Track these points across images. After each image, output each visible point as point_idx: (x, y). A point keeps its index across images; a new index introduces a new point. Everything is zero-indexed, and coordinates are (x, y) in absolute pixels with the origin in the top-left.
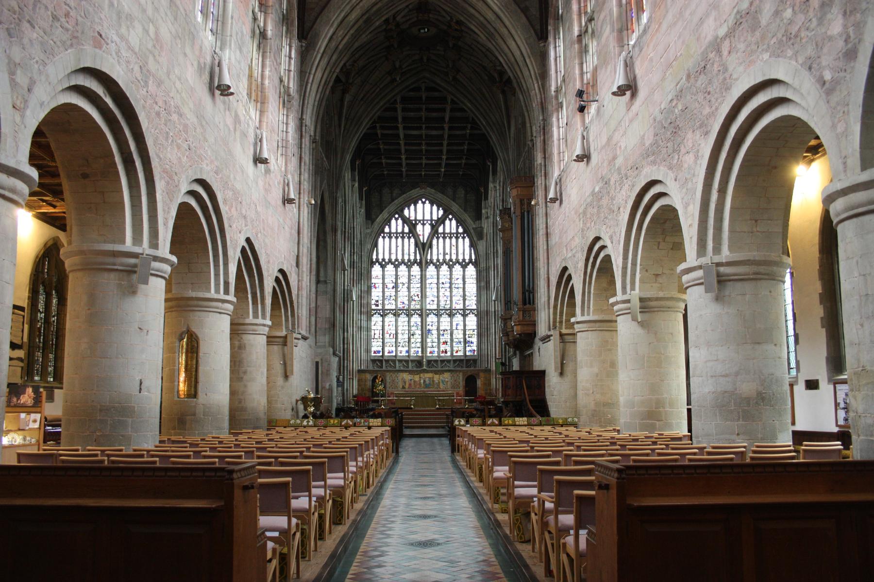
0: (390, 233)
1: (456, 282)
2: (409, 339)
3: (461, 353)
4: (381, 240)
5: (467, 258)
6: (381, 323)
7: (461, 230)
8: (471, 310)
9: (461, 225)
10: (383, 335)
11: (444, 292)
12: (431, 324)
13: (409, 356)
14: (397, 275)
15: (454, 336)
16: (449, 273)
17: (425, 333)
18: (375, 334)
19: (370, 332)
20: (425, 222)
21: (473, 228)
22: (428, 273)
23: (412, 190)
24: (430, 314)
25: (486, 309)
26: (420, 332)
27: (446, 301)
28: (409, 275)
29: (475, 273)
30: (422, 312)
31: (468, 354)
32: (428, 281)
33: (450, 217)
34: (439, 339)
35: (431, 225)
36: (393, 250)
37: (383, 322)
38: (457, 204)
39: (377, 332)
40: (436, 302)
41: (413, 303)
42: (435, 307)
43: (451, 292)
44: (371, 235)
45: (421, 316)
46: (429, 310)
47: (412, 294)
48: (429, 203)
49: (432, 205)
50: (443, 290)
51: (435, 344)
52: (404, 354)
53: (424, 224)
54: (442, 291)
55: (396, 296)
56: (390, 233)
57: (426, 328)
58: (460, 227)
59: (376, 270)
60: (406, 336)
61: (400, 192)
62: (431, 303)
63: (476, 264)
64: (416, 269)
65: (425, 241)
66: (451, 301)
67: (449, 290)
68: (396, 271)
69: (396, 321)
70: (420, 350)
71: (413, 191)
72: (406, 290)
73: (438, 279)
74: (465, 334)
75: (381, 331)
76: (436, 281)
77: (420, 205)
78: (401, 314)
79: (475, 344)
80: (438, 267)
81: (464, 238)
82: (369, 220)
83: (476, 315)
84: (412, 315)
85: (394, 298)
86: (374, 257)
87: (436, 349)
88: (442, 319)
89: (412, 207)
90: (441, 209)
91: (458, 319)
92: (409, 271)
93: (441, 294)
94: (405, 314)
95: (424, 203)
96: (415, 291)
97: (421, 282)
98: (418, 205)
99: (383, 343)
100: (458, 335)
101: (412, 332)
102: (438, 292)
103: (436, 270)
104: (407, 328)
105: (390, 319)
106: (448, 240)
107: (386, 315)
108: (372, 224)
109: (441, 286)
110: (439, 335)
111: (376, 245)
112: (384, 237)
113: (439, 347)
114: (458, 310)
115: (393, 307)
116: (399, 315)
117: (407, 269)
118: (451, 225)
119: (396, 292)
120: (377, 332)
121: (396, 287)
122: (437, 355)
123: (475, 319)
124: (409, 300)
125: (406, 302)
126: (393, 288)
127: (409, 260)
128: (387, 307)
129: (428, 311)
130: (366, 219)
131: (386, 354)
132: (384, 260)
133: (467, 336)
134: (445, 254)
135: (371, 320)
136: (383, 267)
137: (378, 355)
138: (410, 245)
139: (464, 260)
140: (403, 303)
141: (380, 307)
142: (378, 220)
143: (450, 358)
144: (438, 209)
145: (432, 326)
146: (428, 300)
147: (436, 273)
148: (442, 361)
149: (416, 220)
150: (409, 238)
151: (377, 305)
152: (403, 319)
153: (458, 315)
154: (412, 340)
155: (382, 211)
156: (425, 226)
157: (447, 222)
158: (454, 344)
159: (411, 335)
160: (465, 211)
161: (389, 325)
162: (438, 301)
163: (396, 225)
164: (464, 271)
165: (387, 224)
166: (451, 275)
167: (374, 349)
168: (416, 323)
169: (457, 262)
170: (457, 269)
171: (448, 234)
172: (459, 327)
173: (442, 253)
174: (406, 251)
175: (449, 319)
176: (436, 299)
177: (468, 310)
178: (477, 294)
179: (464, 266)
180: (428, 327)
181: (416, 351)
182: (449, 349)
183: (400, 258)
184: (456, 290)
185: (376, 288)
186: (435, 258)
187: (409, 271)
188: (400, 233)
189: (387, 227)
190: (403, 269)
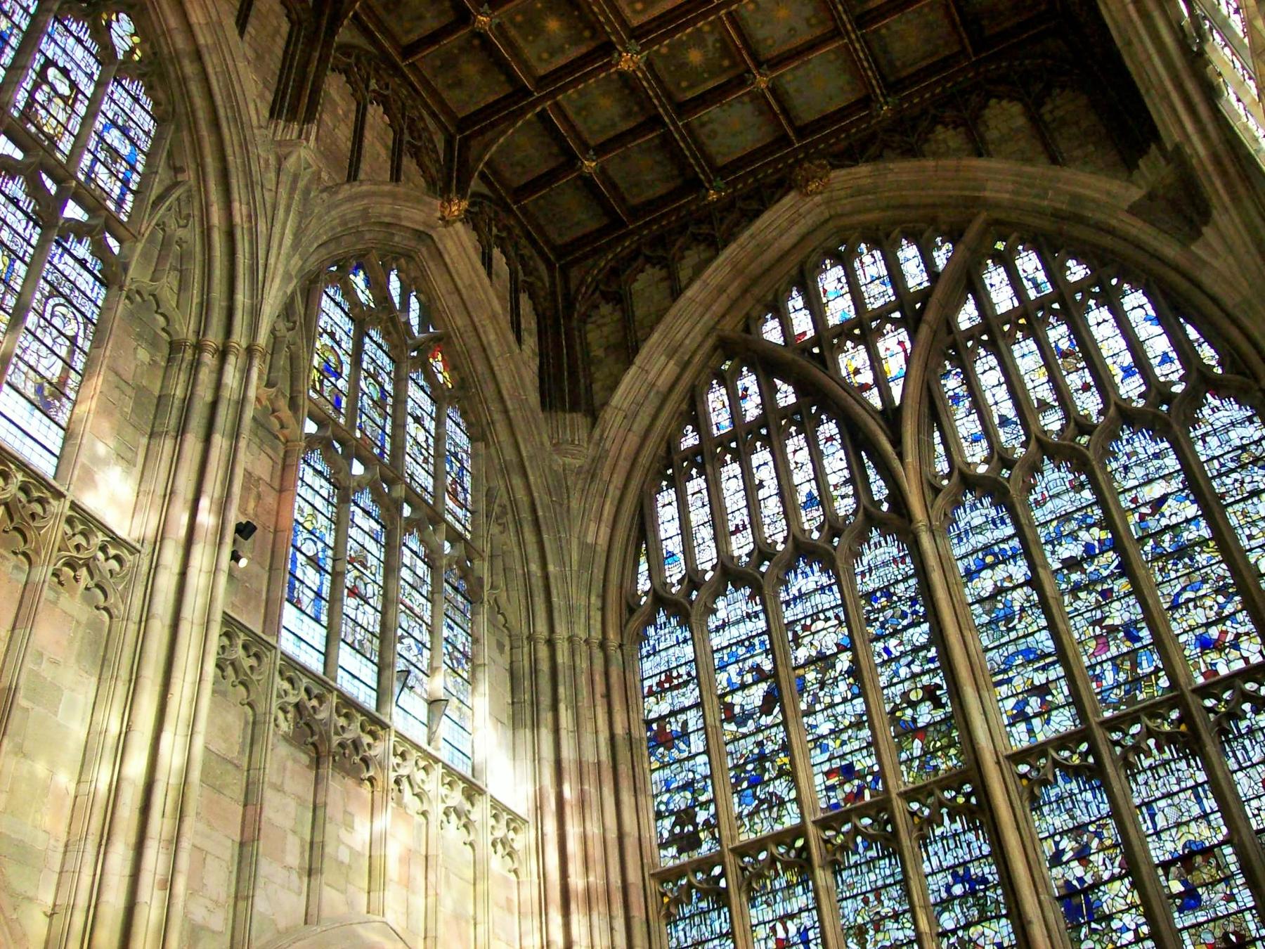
1: (1153, 524)
16: (1087, 494)
21: (1134, 210)
23: (757, 214)
27: (1132, 655)
30: (982, 790)
40: (1061, 694)
50: (1088, 599)
53: (868, 339)
62: (1034, 704)
71: (766, 217)
73: (1028, 552)
77: (831, 279)
82: (574, 408)
93: (1080, 629)
96: (903, 672)
106: (1026, 356)
108: (593, 425)
111: (644, 527)
114: (1232, 680)
126: (766, 709)
129: (1023, 768)
140: (848, 772)
142: (617, 398)
145: (1082, 856)
147: (1010, 530)
155: (636, 350)
160: (1054, 160)
168: (959, 873)
173: (1011, 413)
176: (1060, 670)
184: (1177, 570)
186: (976, 454)
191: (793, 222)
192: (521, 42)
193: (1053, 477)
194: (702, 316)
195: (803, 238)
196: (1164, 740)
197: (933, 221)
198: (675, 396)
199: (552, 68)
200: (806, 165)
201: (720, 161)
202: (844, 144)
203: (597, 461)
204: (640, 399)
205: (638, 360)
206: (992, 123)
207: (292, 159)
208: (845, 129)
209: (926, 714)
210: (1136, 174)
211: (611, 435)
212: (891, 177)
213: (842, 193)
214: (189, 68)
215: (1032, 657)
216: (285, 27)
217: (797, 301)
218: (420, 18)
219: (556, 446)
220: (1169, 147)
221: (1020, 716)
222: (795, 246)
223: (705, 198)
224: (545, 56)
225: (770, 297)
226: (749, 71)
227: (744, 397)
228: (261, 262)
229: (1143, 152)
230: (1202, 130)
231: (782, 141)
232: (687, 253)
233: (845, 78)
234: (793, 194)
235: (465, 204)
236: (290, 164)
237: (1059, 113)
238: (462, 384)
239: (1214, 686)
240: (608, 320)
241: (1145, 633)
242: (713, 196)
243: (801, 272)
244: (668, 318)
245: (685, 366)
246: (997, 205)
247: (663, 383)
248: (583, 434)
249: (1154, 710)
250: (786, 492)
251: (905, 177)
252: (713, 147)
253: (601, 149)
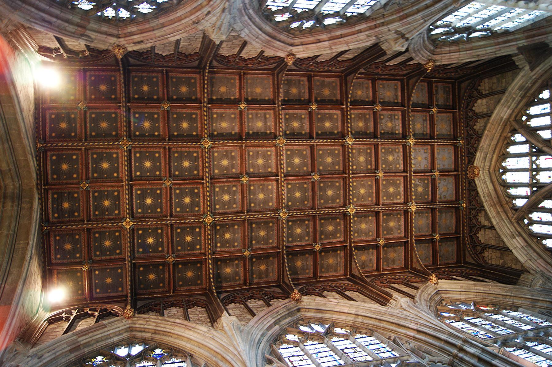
20: (534, 166)
21: (532, 69)
23: (477, 193)
33: (524, 118)
38: (495, 108)
48: (504, 160)
49: (506, 156)
53: (538, 170)
58: (541, 96)
61: (483, 213)
71: (479, 190)
77: (509, 178)
82: (519, 276)
89: (513, 191)
90: (512, 138)
95: (506, 170)
98: (508, 181)
144: (514, 143)
155: (508, 248)
157: (534, 123)
160: (503, 92)
165: (539, 243)
189: (544, 242)
191: (485, 183)
192: (392, 236)
194: (505, 222)
195: (492, 182)
197: (506, 138)
198: (530, 242)
199: (403, 231)
200: (468, 172)
201: (454, 199)
202: (466, 159)
203: (543, 275)
204: (526, 253)
205: (511, 248)
206: (481, 110)
207: (403, 304)
208: (462, 156)
210: (521, 67)
211: (535, 267)
212: (485, 147)
213: (482, 164)
214: (360, 319)
216: (357, 293)
217: (513, 191)
218: (371, 260)
219: (530, 287)
220: (517, 52)
222: (494, 185)
223: (464, 208)
224: (399, 231)
225: (507, 199)
226: (432, 176)
227: (541, 219)
228: (433, 326)
229: (514, 63)
230: (516, 40)
231: (456, 176)
232: (479, 220)
233: (446, 150)
234: (476, 179)
235: (434, 275)
236: (404, 306)
237: (487, 88)
238: (494, 305)
240: (490, 255)
242: (464, 205)
243: (504, 186)
244: (500, 233)
245: (520, 235)
246: (511, 115)
247: (523, 243)
248: (530, 277)
251: (487, 142)
252: (448, 198)
253: (434, 231)
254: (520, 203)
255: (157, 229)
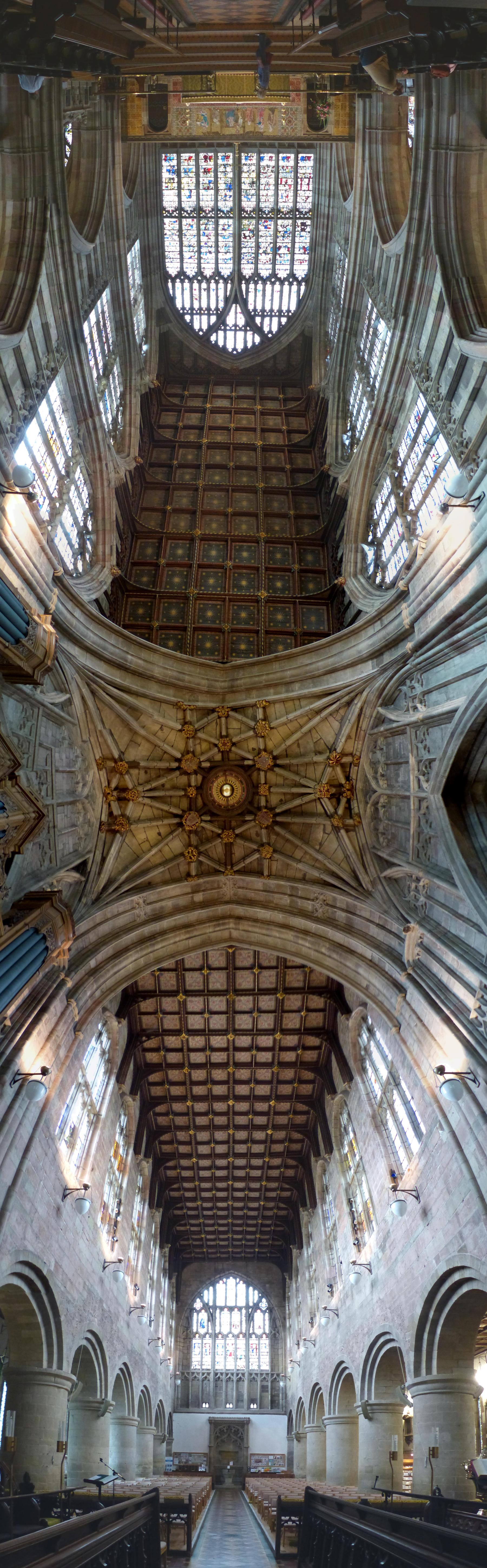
0: (280, 316)
1: (192, 254)
2: (258, 177)
3: (185, 156)
4: (293, 308)
5: (178, 284)
6: (299, 199)
7: (188, 318)
8: (171, 217)
9: (187, 324)
10: (297, 183)
11: (208, 240)
12: (228, 198)
13: (259, 153)
14: (274, 262)
15: (194, 180)
16: (203, 265)
17: (236, 186)
18: (308, 184)
19: (314, 188)
22: (231, 266)
24: (228, 211)
25: (149, 220)
26: (244, 187)
28: (256, 264)
29: (167, 265)
30: (240, 214)
31: (175, 156)
32: (230, 255)
33: (201, 333)
34: (216, 177)
35: (225, 325)
36: (277, 296)
37: (295, 202)
39: (305, 187)
40: (220, 228)
41: (251, 227)
42: (222, 222)
43: (199, 241)
44: (306, 317)
45: (241, 209)
46: (230, 218)
47: (253, 240)
50: (210, 244)
51: (221, 169)
52: (266, 156)
53: (236, 325)
54: (212, 242)
55: (276, 237)
56: (280, 316)
57: (234, 193)
59: (301, 270)
60: (263, 181)
62: (226, 227)
63: (166, 276)
64: (247, 270)
65: (234, 305)
66: (199, 229)
67: (202, 244)
68: (274, 269)
69: (276, 202)
70: (243, 161)
72: (262, 245)
73: (217, 259)
74: (179, 183)
75: (299, 188)
76: (220, 256)
77: (240, 347)
78: (269, 212)
79: (164, 170)
80: (217, 274)
81: (183, 308)
83: (164, 209)
84: (254, 210)
85: (279, 235)
86: (303, 288)
87: (220, 162)
88: (212, 204)
89: (249, 345)
91: (188, 204)
92: (256, 269)
93: (213, 239)
94: (264, 212)
97: (240, 254)
99: (296, 172)
100: (188, 182)
101: (255, 186)
102: (217, 241)
103: (220, 270)
104: (262, 192)
105: (285, 205)
107: (291, 211)
109: (213, 250)
110: (216, 182)
111: (300, 302)
112: (288, 311)
113: (216, 165)
114: (189, 217)
115: (280, 222)
116: (272, 210)
117: (260, 271)
118: (200, 323)
119: (275, 242)
120: (305, 187)
121: (276, 249)
122: (219, 154)
123: (165, 204)
124: (258, 231)
125: (261, 228)
126: (280, 248)
127: (256, 283)
128: (290, 221)
130: (311, 338)
131: (292, 156)
132: (291, 284)
133: (176, 180)
134: (208, 290)
135: (313, 204)
136: (292, 275)
137: (304, 155)
138: (255, 301)
139: (182, 282)
140: (266, 227)
141: (299, 222)
143: (199, 149)
144: (216, 342)
145: (226, 195)
146: (231, 230)
147: (220, 266)
148: (210, 145)
149: (246, 331)
150: (255, 310)
151: (303, 224)
152: (267, 205)
153: (189, 209)
154: (254, 175)
156: (233, 323)
157: (205, 327)
158: (194, 170)
159: (256, 183)
161: (287, 196)
162: (216, 229)
163: (271, 326)
164: (182, 267)
165: (283, 326)
166: (199, 264)
167: (310, 163)
168: (249, 200)
169: (191, 280)
170: (191, 269)
171: (204, 314)
172: (187, 193)
174: (260, 294)
175: (202, 204)
176: (220, 232)
177: (175, 217)
178: (163, 238)
179: (182, 275)
180: (231, 193)
181: (249, 162)
182: (202, 163)
183: (269, 287)
185: (304, 248)
186: (221, 285)
187: (256, 269)
188: (267, 316)
189: (283, 323)
190: (265, 273)
193: (208, 272)
196: (205, 211)
209: (247, 233)
215: (224, 236)
221: (229, 226)
239: (193, 217)
241: (201, 232)
249: (204, 217)
250: (264, 295)
254: (257, 339)
255: (269, 579)
